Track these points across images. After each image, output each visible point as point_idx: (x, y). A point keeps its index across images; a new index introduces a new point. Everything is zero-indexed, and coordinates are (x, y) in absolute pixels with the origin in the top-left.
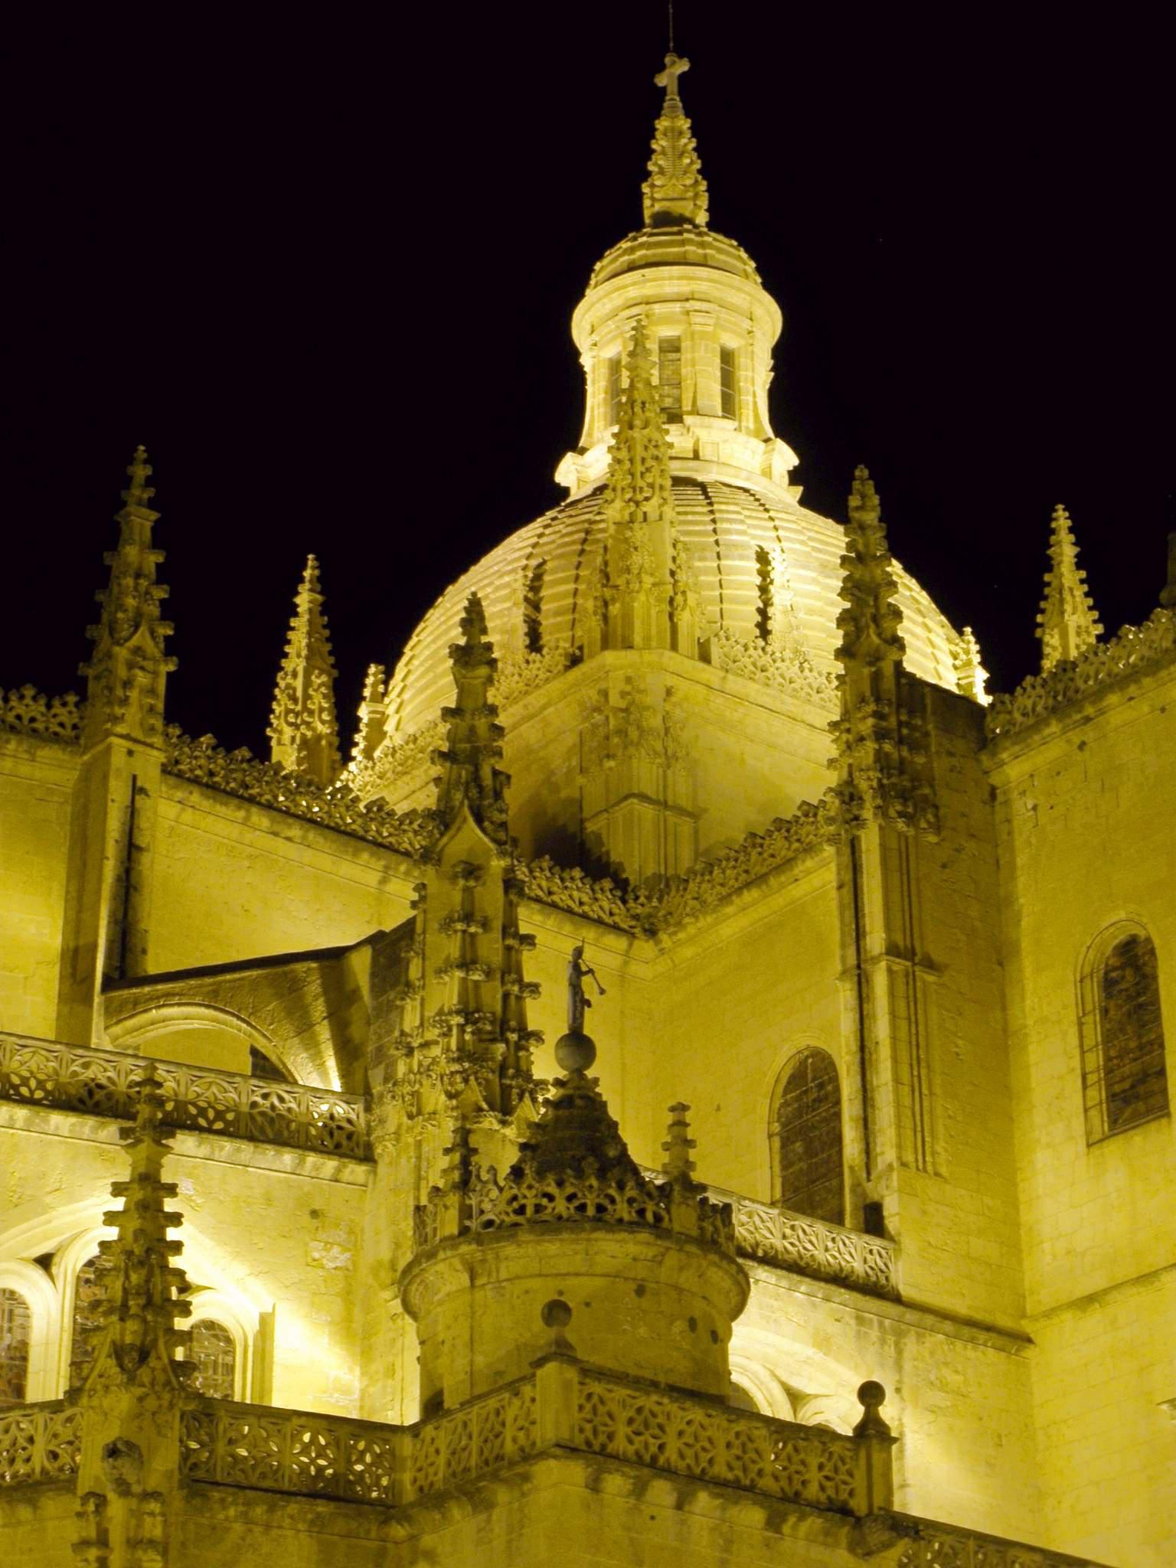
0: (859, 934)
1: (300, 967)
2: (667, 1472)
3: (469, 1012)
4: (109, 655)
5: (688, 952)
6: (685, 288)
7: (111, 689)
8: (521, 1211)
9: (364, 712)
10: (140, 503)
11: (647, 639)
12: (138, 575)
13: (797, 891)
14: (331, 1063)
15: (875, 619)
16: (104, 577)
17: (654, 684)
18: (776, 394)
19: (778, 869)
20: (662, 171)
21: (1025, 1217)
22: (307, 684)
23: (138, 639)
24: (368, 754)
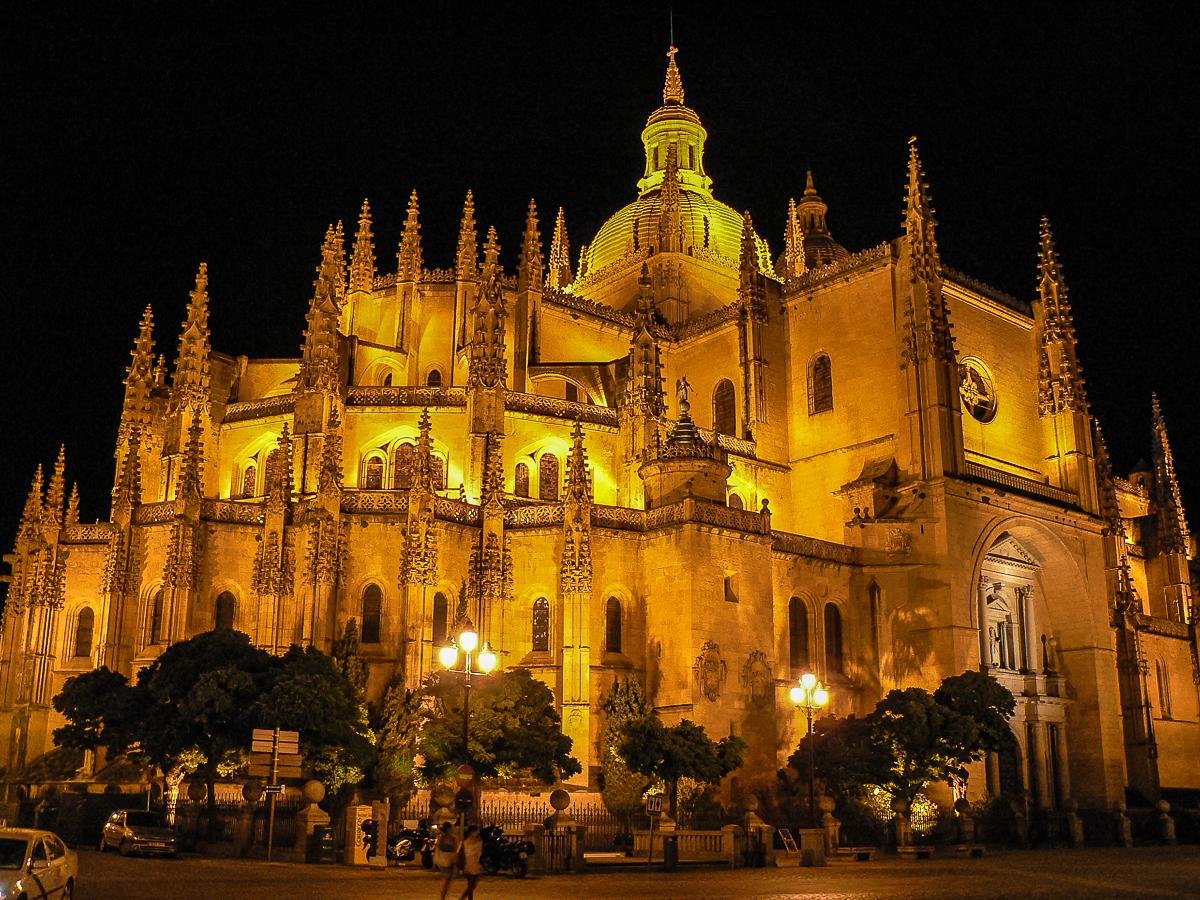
0: (746, 353)
1: (593, 367)
2: (716, 526)
3: (647, 386)
4: (526, 264)
5: (687, 347)
6: (678, 126)
7: (527, 275)
8: (674, 454)
9: (580, 261)
10: (533, 217)
11: (674, 248)
12: (533, 240)
13: (724, 331)
14: (604, 399)
15: (751, 258)
16: (522, 240)
17: (676, 262)
18: (704, 158)
19: (717, 325)
20: (669, 86)
21: (790, 434)
22: (561, 249)
23: (535, 259)
24: (582, 275)
